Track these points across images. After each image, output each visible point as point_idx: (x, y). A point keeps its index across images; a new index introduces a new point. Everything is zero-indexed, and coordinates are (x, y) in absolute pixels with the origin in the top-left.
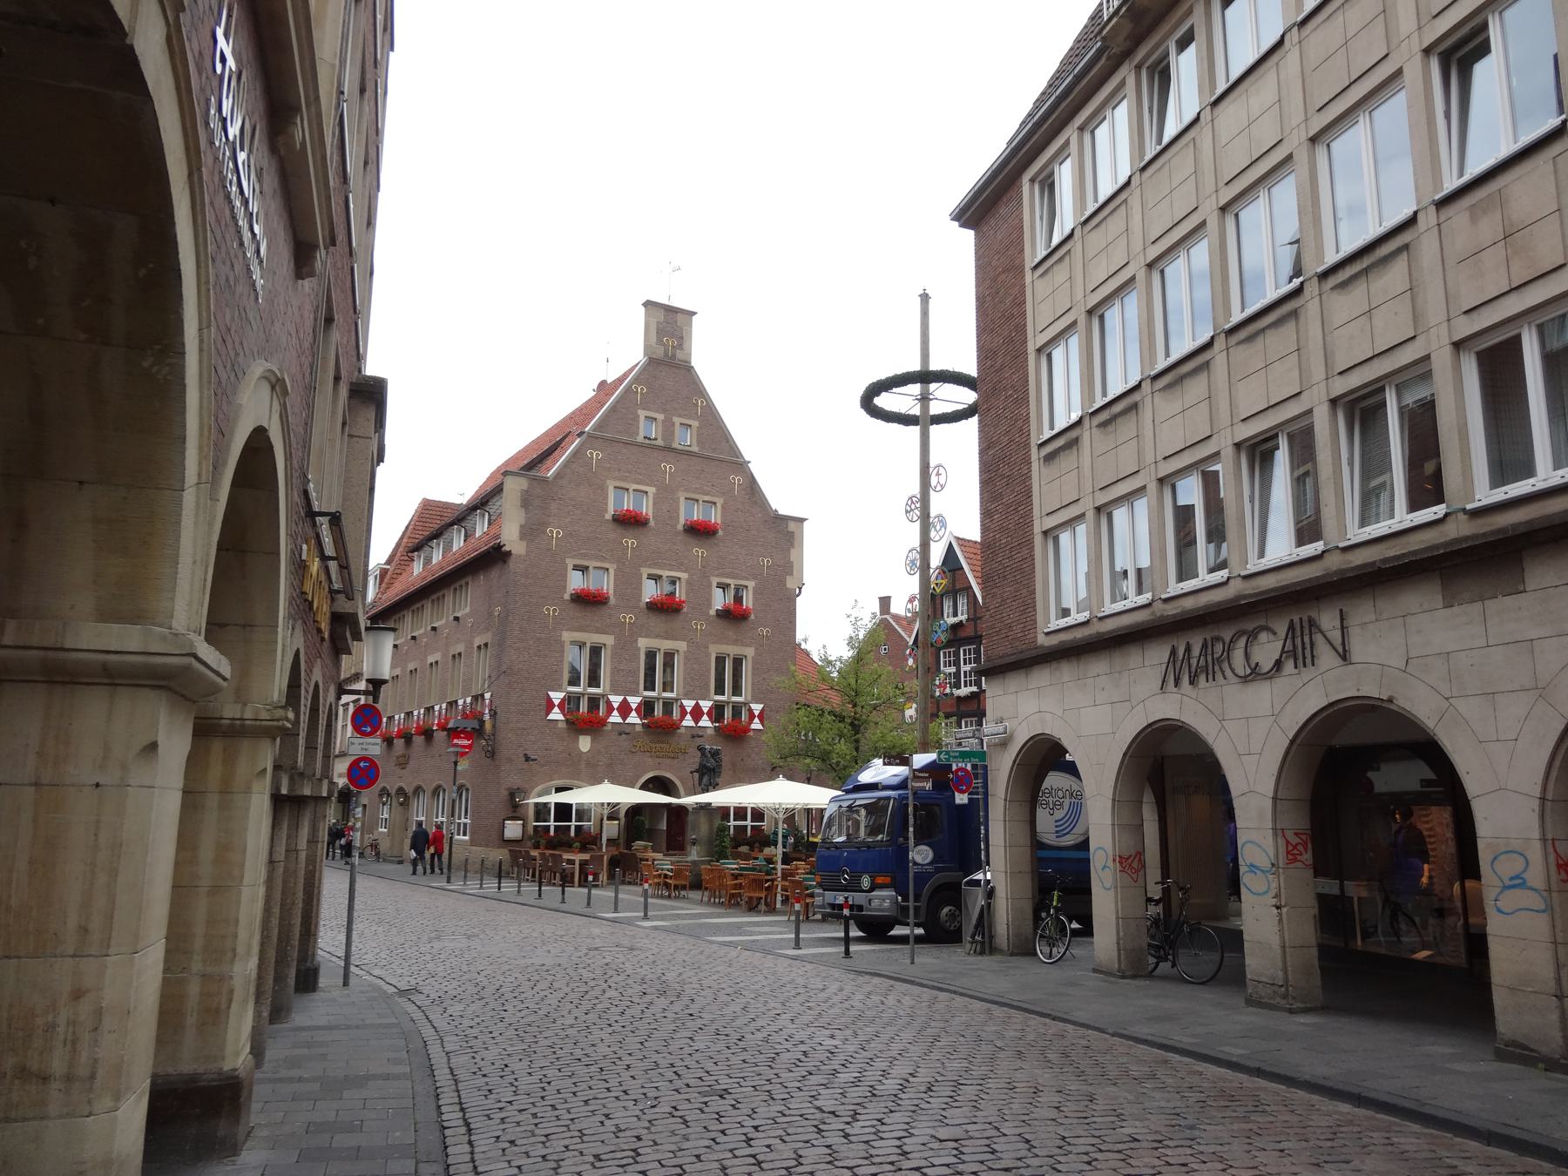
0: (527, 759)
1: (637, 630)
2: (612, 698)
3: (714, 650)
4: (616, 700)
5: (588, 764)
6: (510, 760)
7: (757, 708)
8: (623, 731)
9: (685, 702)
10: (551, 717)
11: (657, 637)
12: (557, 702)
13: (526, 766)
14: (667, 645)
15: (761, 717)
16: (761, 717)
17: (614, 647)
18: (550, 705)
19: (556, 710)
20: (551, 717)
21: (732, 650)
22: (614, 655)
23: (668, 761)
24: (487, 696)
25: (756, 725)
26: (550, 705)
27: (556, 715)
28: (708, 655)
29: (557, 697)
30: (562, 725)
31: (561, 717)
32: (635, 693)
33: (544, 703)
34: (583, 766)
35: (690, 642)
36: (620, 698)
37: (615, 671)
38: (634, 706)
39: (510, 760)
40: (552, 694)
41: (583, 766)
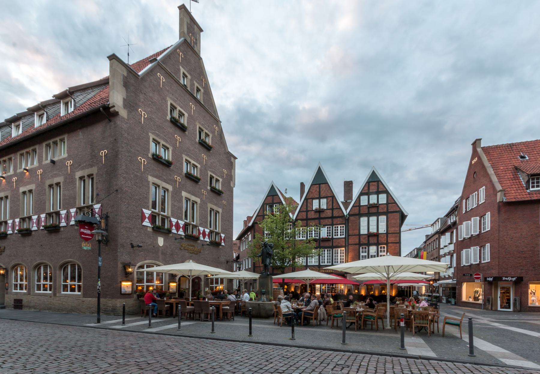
0: (133, 247)
1: (182, 187)
2: (173, 219)
3: (210, 206)
4: (174, 220)
6: (123, 246)
8: (178, 238)
10: (144, 224)
11: (189, 193)
12: (147, 216)
13: (132, 250)
14: (193, 198)
17: (173, 192)
18: (143, 217)
20: (144, 224)
22: (172, 196)
23: (194, 255)
24: (97, 207)
26: (143, 217)
27: (147, 223)
28: (207, 208)
29: (147, 212)
30: (150, 230)
31: (149, 225)
34: (160, 254)
35: (201, 200)
37: (173, 206)
39: (123, 246)
40: (145, 211)
41: (160, 254)
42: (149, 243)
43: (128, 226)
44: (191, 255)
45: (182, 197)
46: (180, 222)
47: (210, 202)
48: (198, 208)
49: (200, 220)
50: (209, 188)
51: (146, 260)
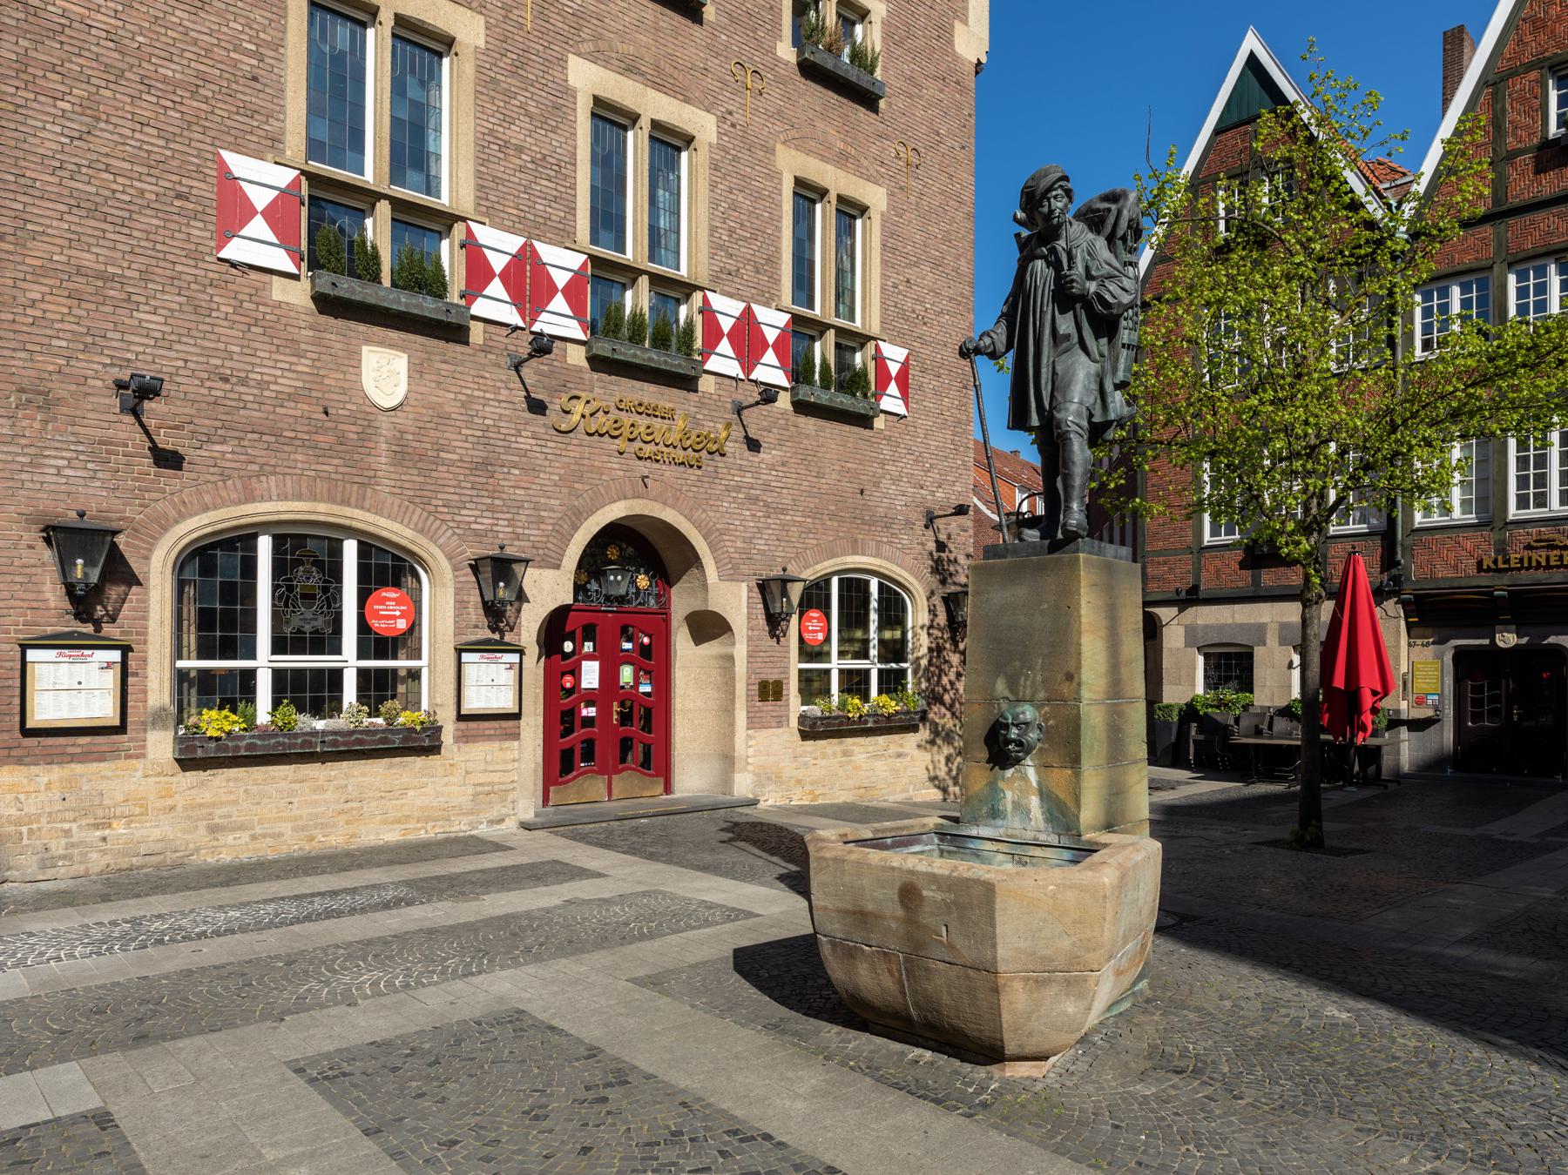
5: (402, 454)
7: (895, 355)
9: (718, 301)
10: (235, 250)
11: (629, 69)
15: (903, 380)
16: (903, 380)
17: (488, 61)
19: (258, 227)
20: (235, 250)
21: (837, 180)
25: (891, 402)
28: (775, 176)
32: (565, 239)
33: (205, 190)
34: (382, 459)
36: (513, 243)
38: (561, 279)
41: (382, 459)
42: (287, 383)
43: (87, 259)
44: (643, 468)
45: (570, 93)
46: (548, 253)
47: (799, 143)
48: (704, 173)
49: (716, 247)
50: (787, 52)
51: (250, 498)
